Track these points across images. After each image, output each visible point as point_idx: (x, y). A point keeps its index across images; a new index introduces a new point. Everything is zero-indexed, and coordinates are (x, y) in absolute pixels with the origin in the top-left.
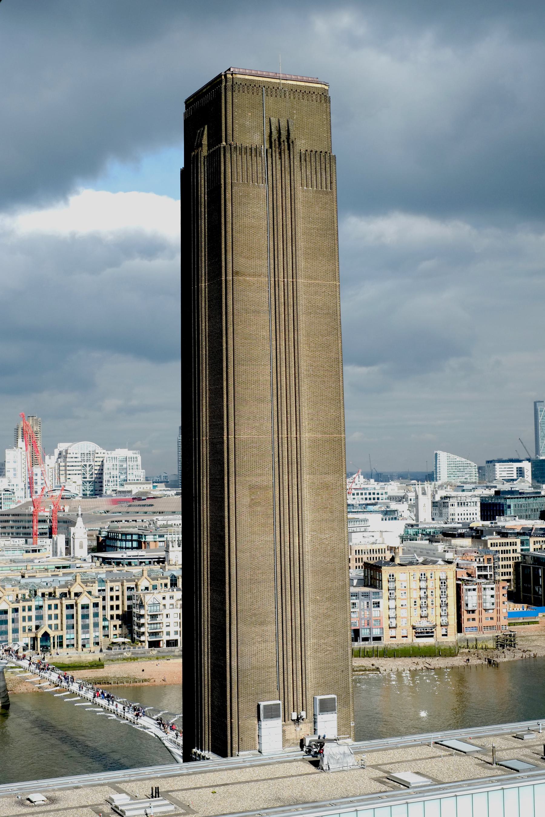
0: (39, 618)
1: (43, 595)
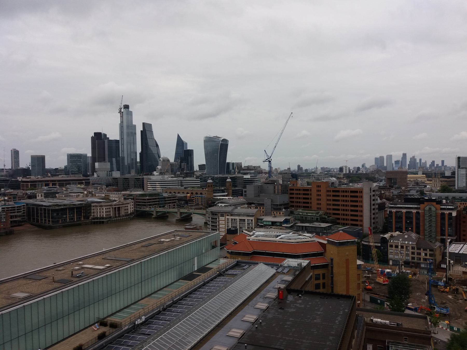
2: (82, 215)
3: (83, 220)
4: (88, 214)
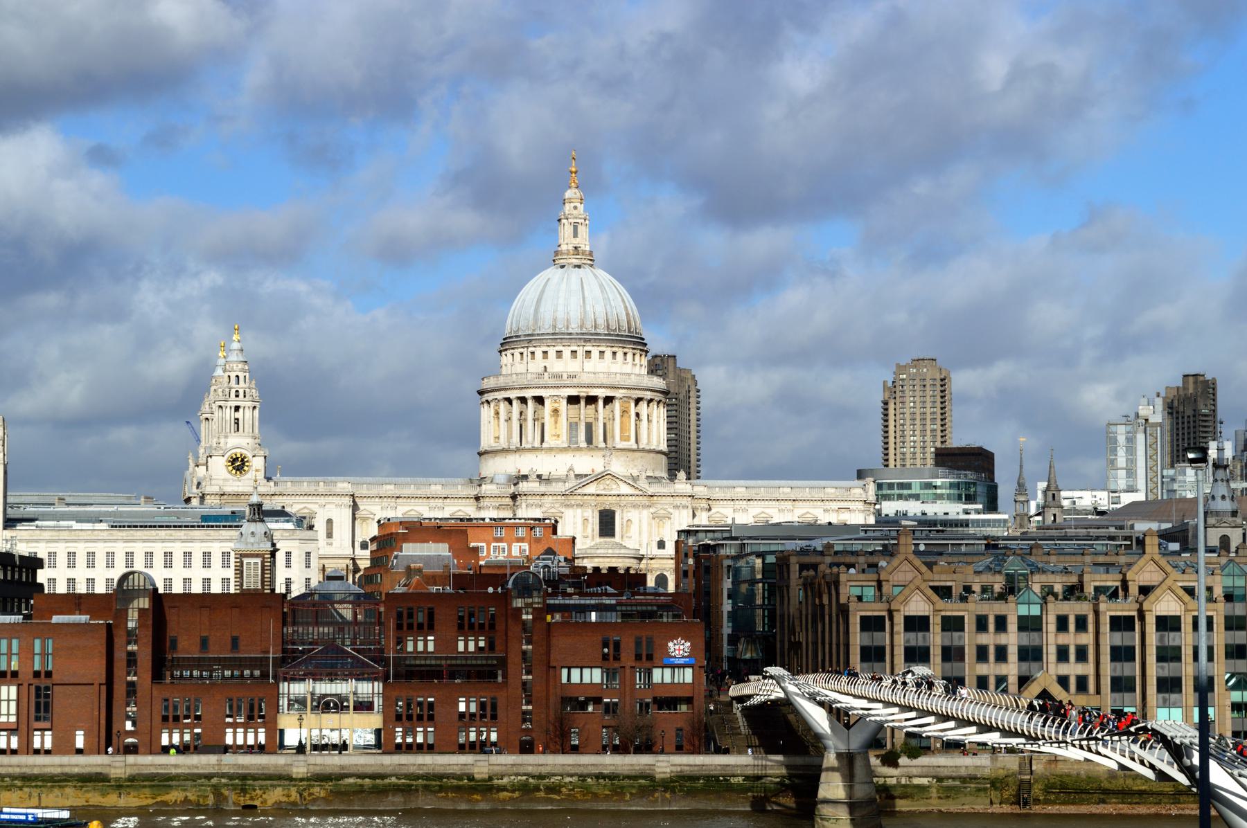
0: (1031, 654)
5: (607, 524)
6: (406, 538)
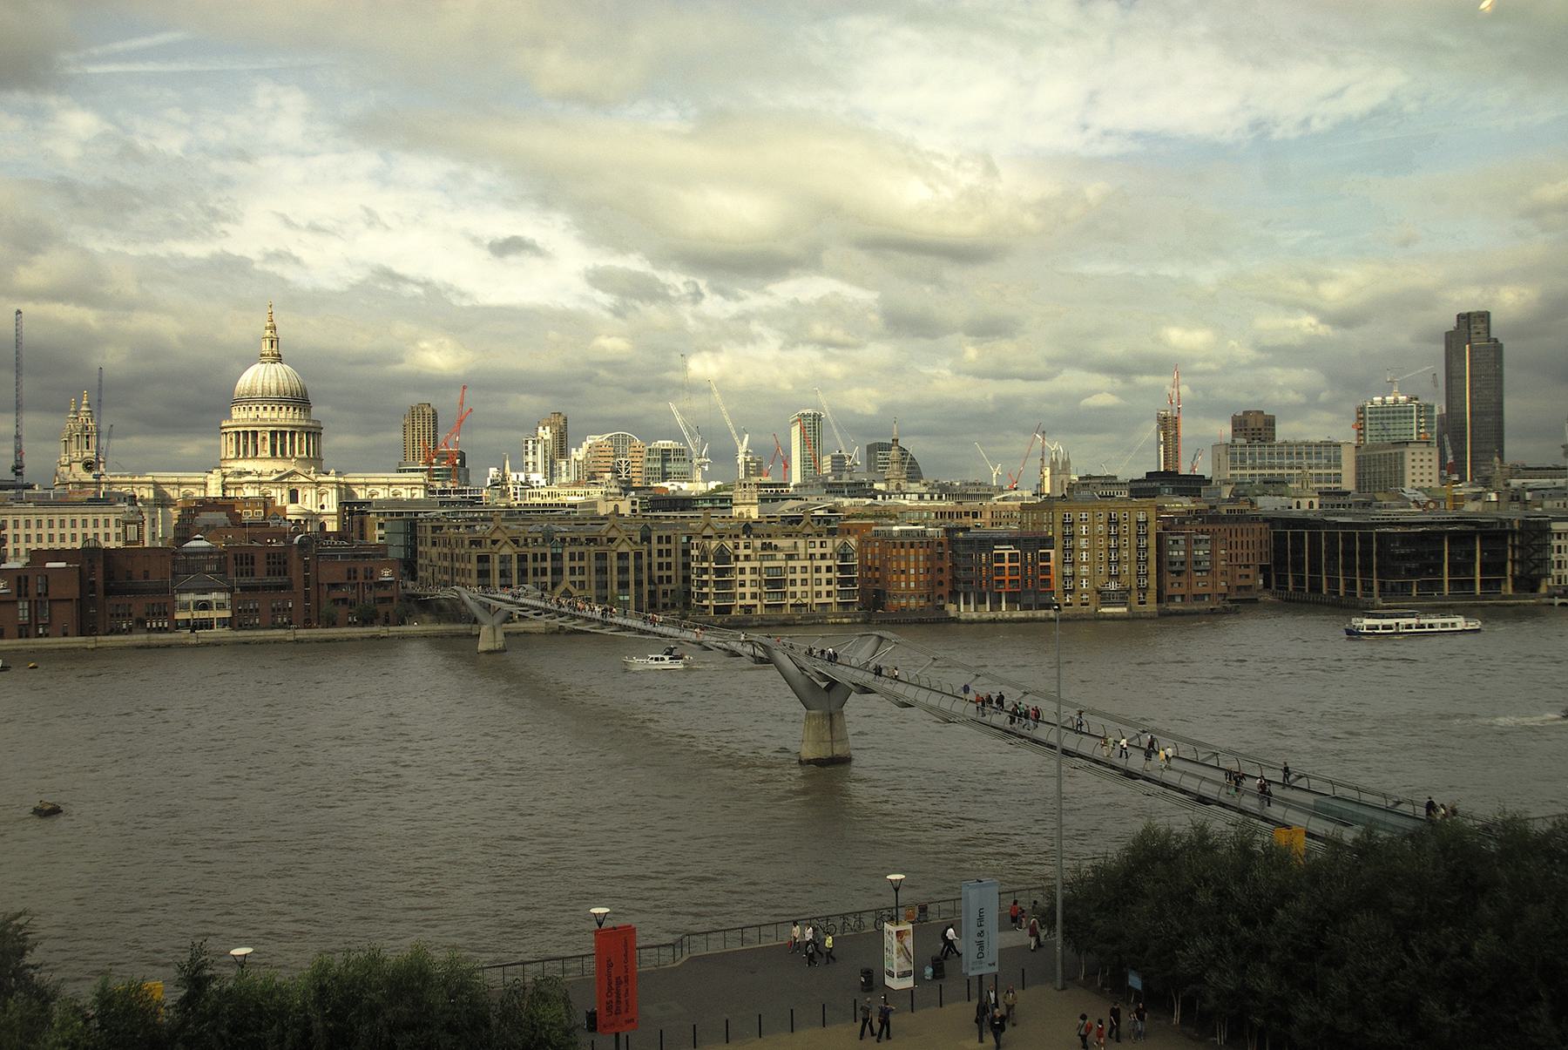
0: (557, 571)
1: (563, 540)
2: (1509, 572)
3: (1510, 592)
4: (1537, 566)
5: (294, 497)
6: (202, 510)
